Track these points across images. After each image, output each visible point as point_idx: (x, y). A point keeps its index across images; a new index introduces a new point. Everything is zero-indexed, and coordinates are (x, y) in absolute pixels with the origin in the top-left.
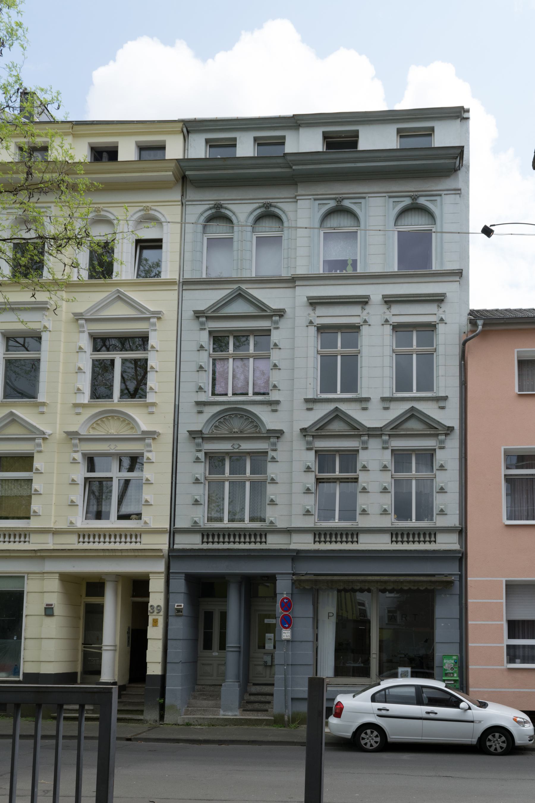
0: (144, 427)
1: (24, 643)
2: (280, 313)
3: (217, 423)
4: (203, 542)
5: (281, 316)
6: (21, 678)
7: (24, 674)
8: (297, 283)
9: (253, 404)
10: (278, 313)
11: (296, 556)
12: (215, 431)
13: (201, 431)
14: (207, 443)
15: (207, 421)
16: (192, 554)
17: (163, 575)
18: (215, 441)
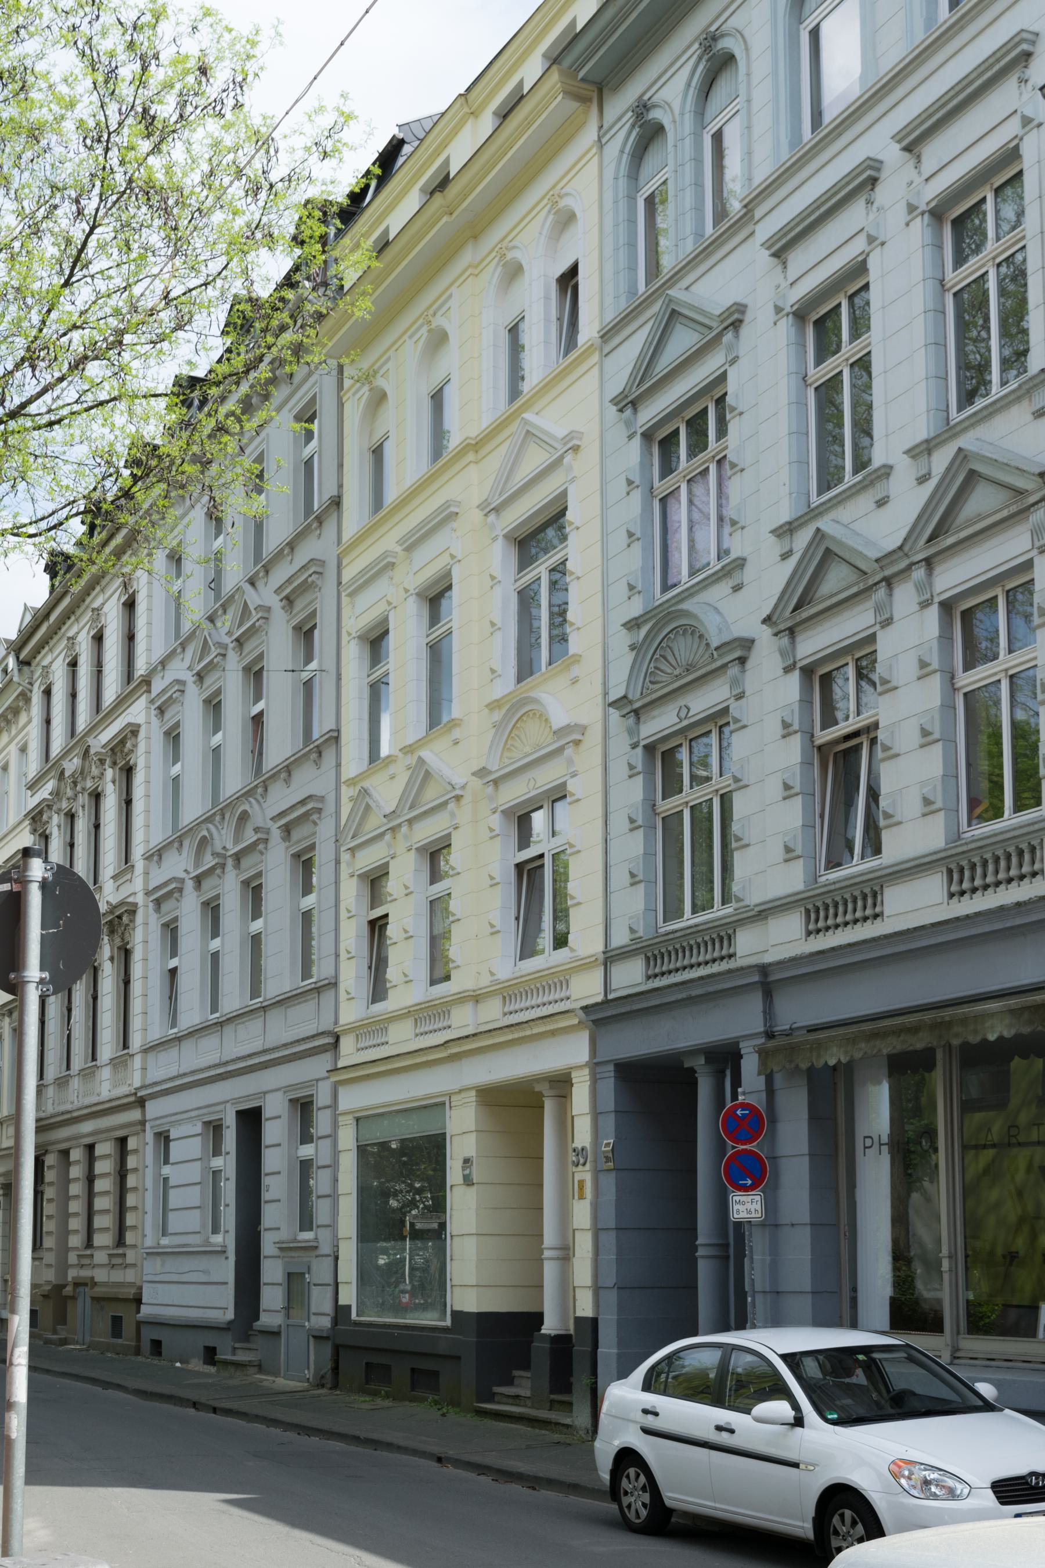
0: (559, 718)
1: (451, 1245)
2: (734, 320)
3: (652, 665)
4: (648, 977)
5: (736, 325)
6: (448, 1322)
7: (456, 1314)
8: (758, 213)
9: (705, 587)
10: (729, 321)
11: (767, 981)
12: (651, 686)
13: (625, 697)
14: (645, 723)
15: (632, 667)
16: (614, 1012)
17: (586, 1071)
18: (656, 712)
